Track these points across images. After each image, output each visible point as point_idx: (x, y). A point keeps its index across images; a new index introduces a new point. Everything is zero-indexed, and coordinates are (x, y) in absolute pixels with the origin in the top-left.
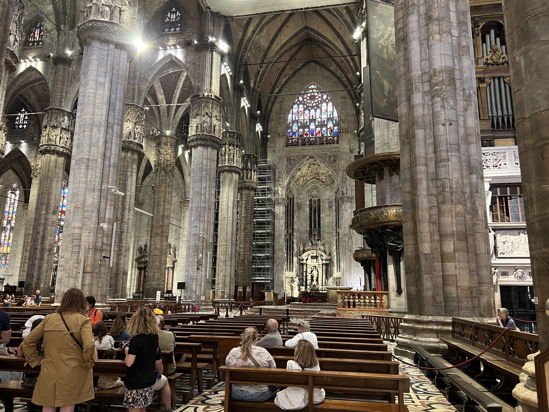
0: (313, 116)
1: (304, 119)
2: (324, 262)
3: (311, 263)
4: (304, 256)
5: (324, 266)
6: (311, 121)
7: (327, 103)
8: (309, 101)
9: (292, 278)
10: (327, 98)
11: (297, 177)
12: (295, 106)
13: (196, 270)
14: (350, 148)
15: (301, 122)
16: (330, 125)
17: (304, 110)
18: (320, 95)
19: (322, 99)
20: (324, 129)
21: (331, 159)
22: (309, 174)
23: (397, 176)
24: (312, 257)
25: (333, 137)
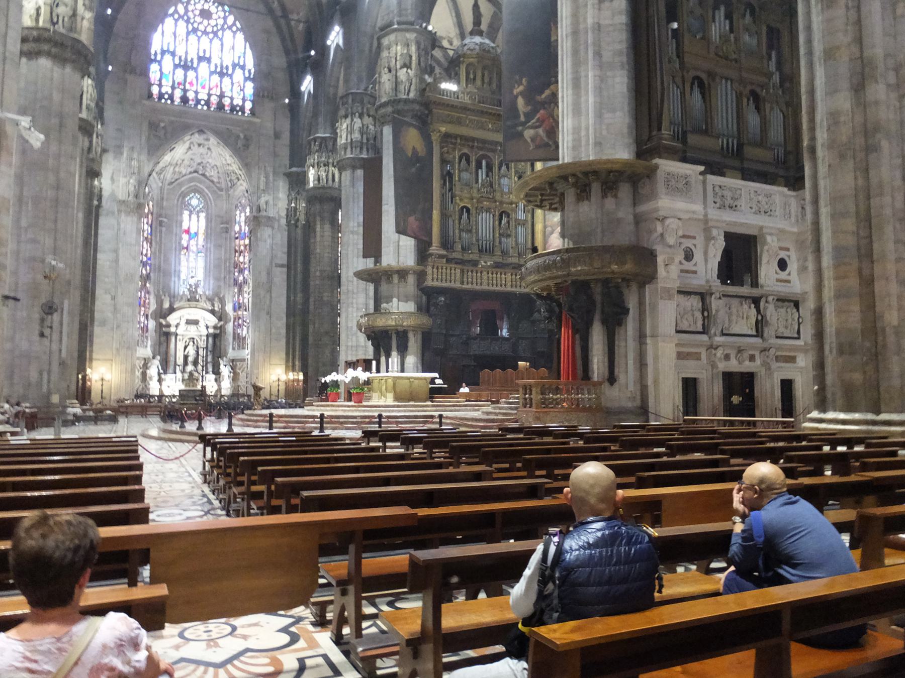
0: (204, 51)
1: (187, 53)
2: (211, 331)
3: (184, 332)
4: (173, 319)
5: (210, 340)
6: (201, 59)
7: (235, 33)
8: (198, 19)
9: (145, 359)
10: (234, 24)
11: (161, 165)
12: (169, 21)
13: (36, 337)
14: (275, 129)
15: (180, 58)
16: (239, 75)
17: (188, 33)
18: (222, 14)
19: (225, 23)
20: (226, 80)
21: (240, 144)
22: (186, 162)
23: (613, 200)
24: (189, 322)
25: (244, 100)
